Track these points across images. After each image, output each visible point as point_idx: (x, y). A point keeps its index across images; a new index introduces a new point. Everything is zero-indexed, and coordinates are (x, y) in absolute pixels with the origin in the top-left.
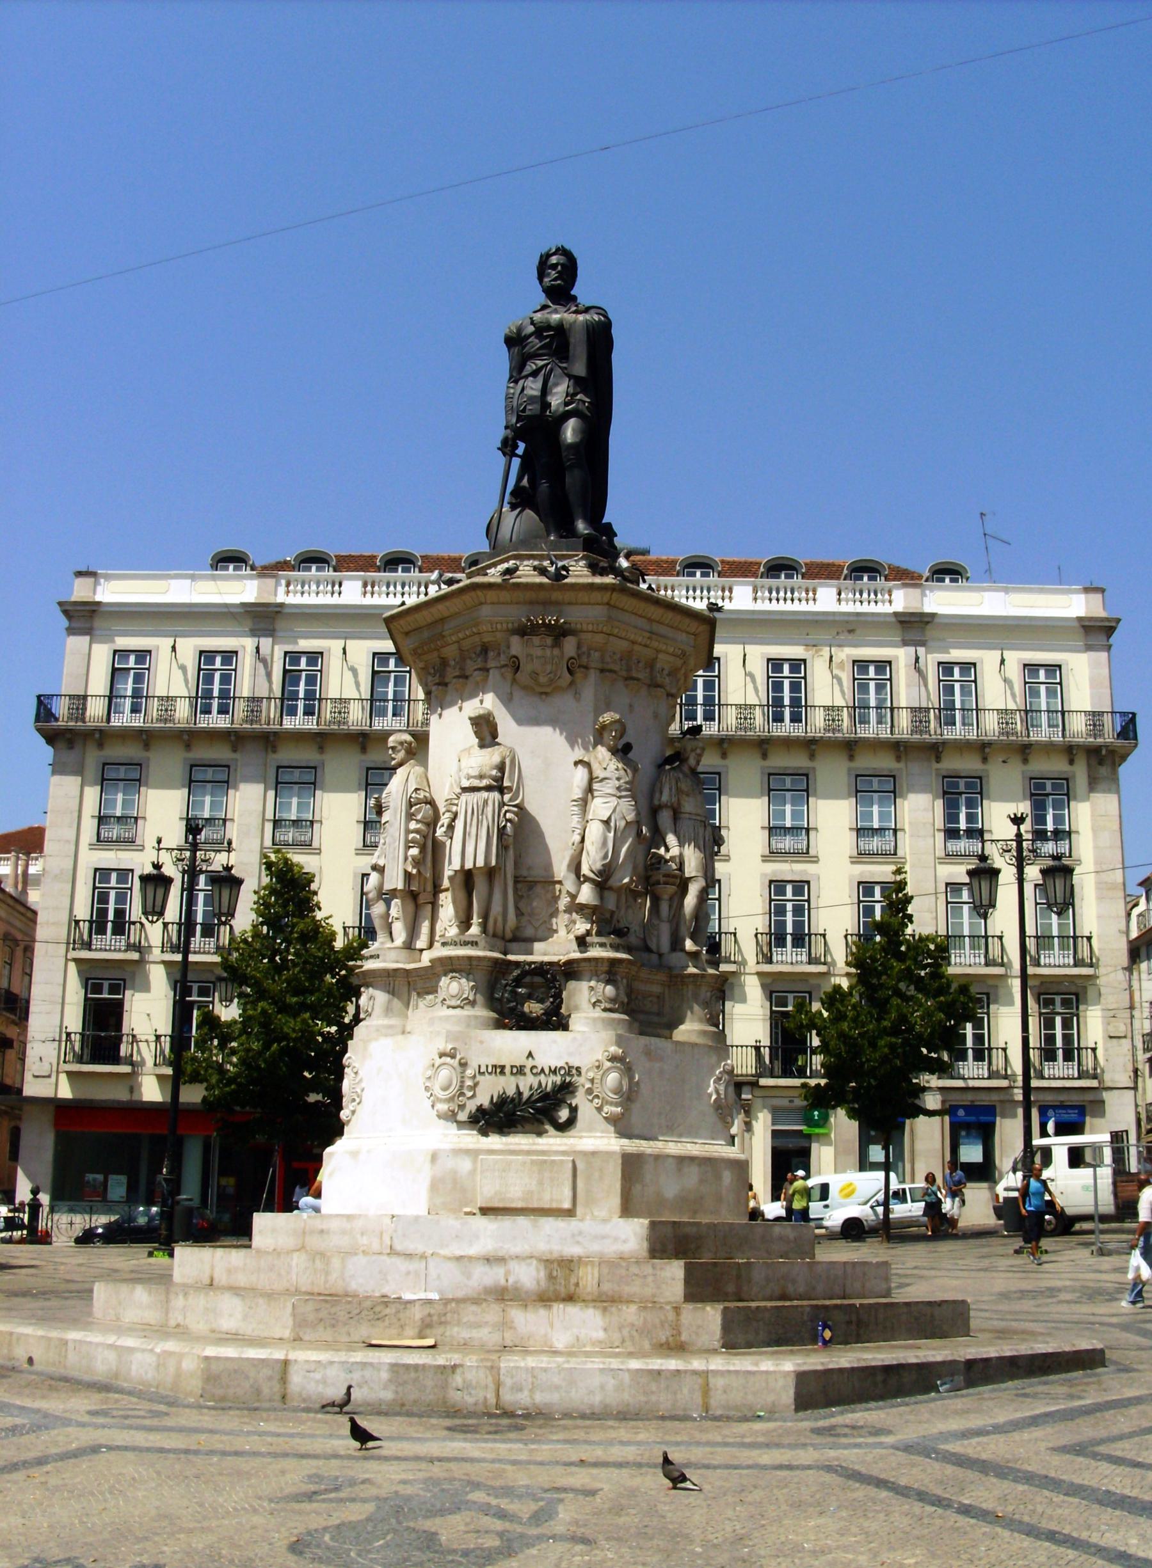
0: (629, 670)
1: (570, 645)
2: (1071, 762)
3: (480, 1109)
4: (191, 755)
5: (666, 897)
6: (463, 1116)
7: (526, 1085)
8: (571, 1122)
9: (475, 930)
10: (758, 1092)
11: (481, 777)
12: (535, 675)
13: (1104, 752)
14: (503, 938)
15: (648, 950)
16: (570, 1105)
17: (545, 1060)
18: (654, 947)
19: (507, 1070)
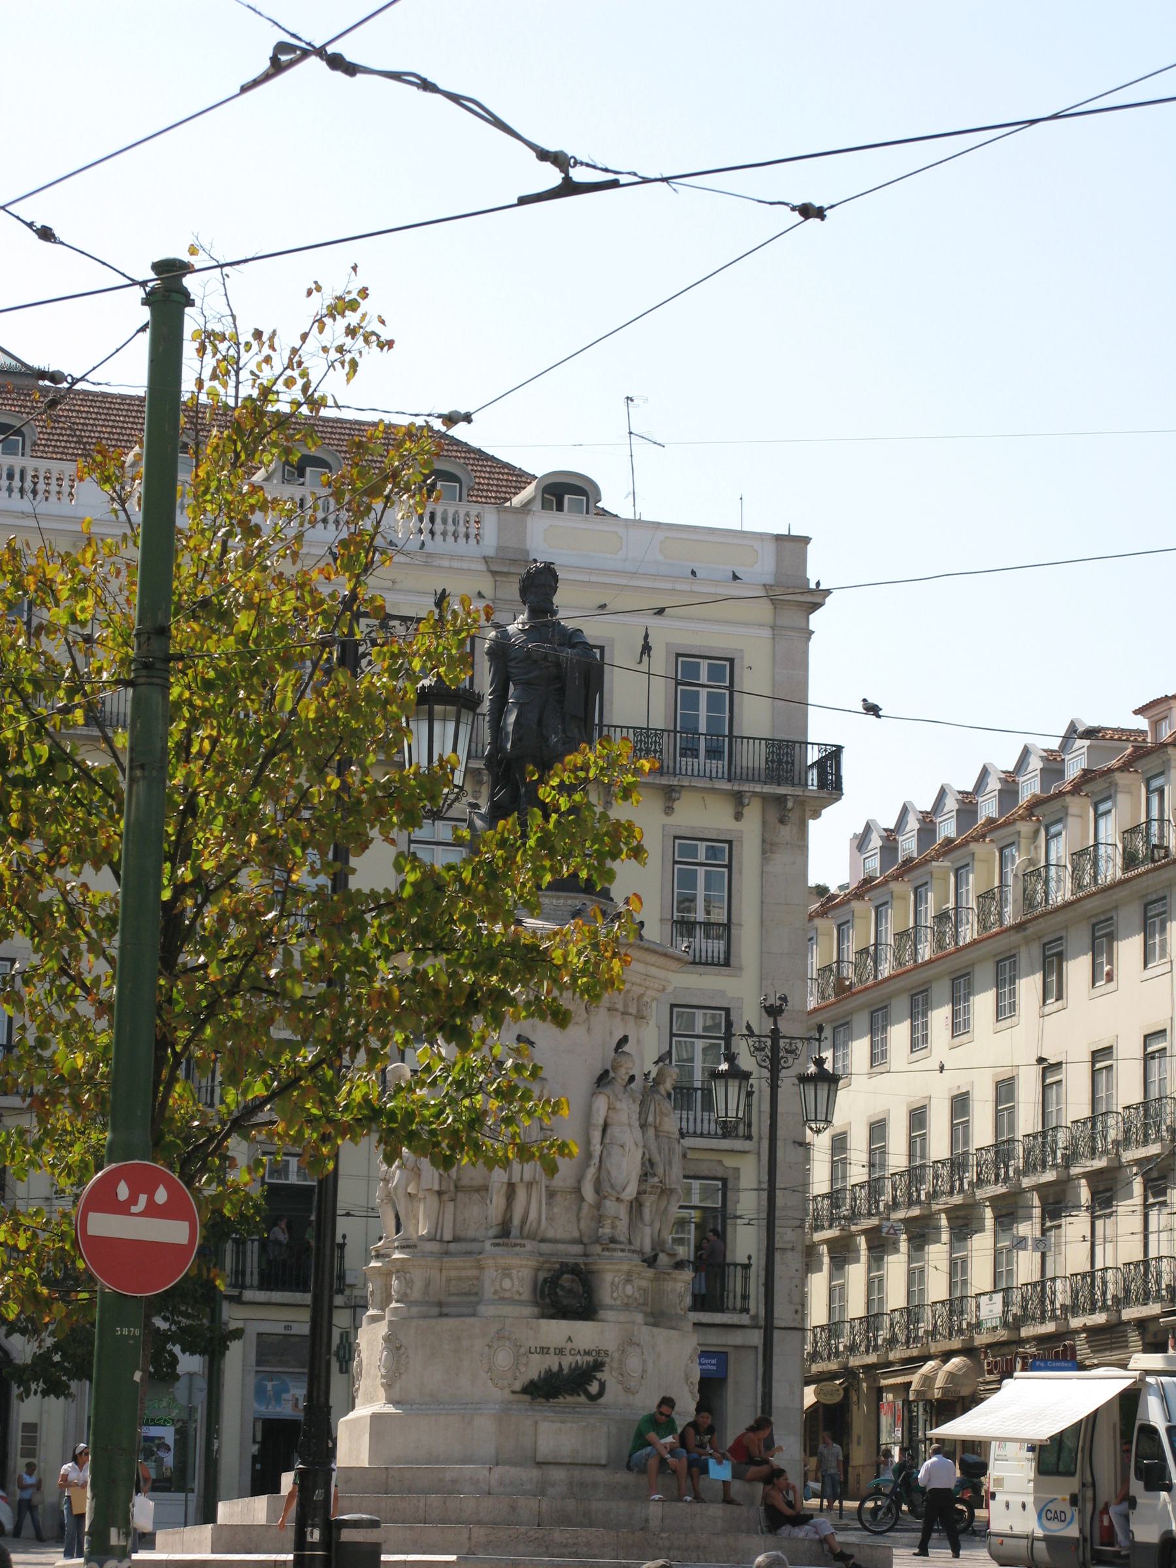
2: (738, 816)
3: (532, 1382)
5: (648, 1204)
6: (518, 1386)
7: (567, 1361)
8: (601, 1393)
13: (790, 805)
16: (600, 1380)
19: (552, 1351)
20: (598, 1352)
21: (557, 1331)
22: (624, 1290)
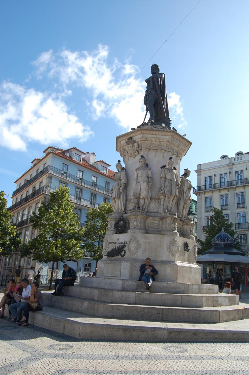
5: (162, 199)
7: (117, 245)
17: (121, 240)
18: (160, 213)
20: (124, 243)
22: (133, 223)
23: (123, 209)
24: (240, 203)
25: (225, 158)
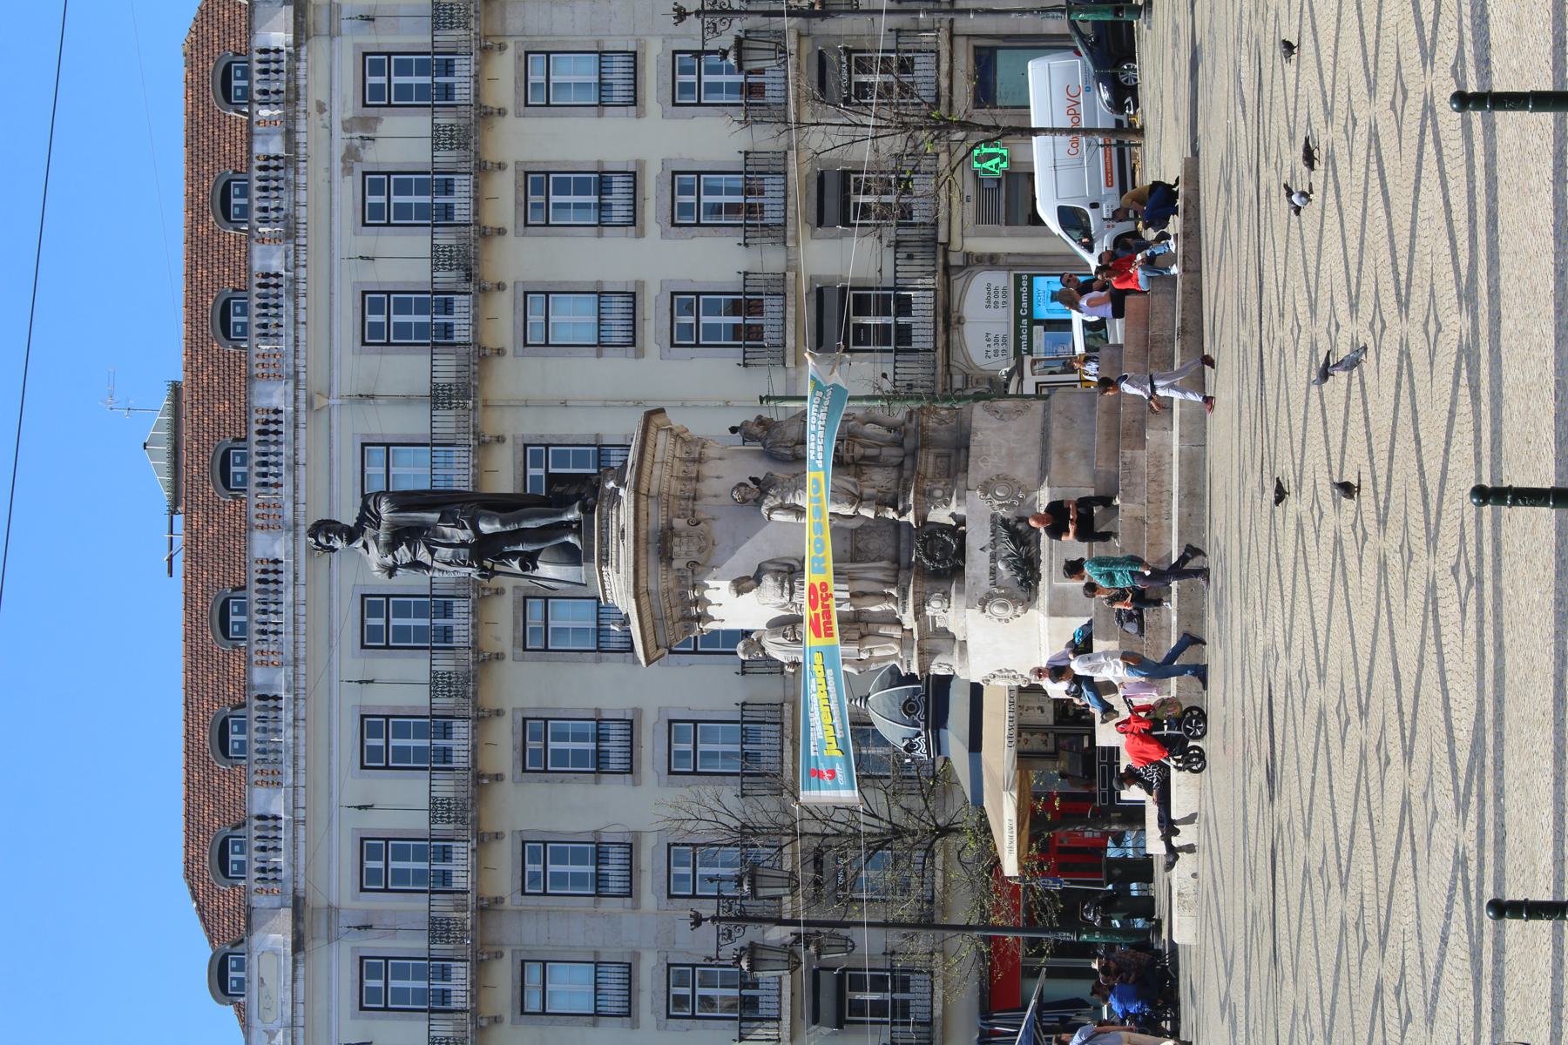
0: (691, 479)
1: (679, 523)
4: (507, 1017)
9: (894, 592)
10: (956, 244)
11: (782, 587)
12: (701, 550)
14: (898, 570)
15: (900, 466)
17: (987, 539)
21: (977, 563)
23: (884, 564)
24: (597, 874)
25: (241, 966)
